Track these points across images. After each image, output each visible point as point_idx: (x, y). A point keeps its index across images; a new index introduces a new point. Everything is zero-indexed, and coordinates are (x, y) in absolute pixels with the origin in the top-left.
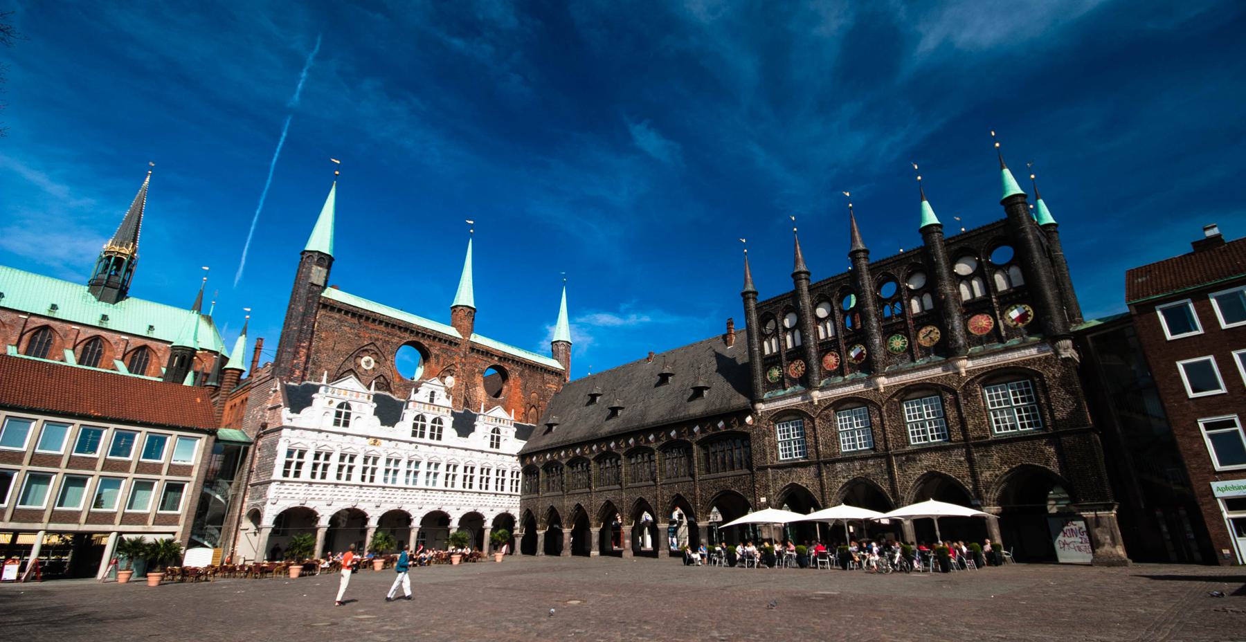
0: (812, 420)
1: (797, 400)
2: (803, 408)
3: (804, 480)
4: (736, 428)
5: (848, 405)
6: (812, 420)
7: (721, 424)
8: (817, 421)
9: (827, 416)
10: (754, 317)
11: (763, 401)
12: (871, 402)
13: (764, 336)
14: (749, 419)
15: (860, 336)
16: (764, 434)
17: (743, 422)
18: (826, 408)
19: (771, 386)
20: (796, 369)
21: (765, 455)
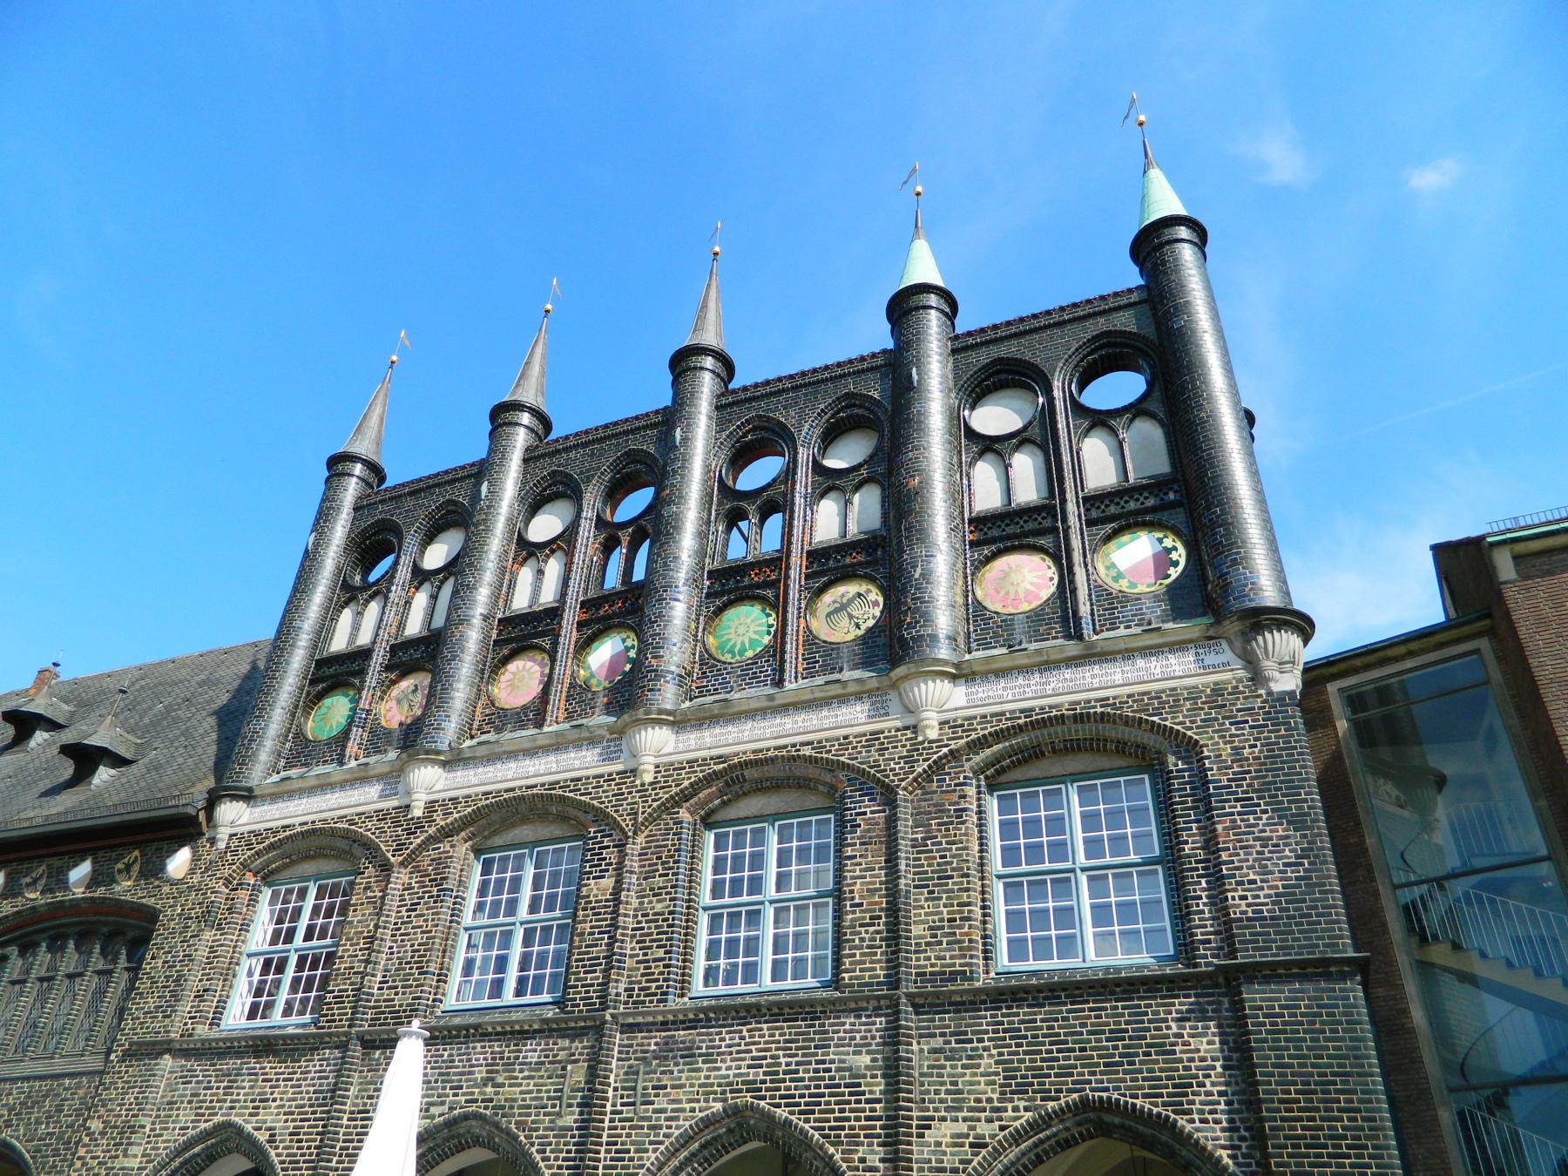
0: (386, 868)
1: (368, 797)
2: (367, 830)
3: (271, 1117)
4: (125, 888)
5: (525, 832)
6: (386, 868)
7: (81, 872)
8: (400, 877)
9: (441, 863)
10: (339, 532)
11: (248, 796)
12: (600, 816)
13: (349, 593)
14: (179, 862)
15: (630, 608)
16: (207, 917)
17: (153, 870)
18: (447, 833)
19: (301, 750)
20: (395, 706)
21: (176, 997)
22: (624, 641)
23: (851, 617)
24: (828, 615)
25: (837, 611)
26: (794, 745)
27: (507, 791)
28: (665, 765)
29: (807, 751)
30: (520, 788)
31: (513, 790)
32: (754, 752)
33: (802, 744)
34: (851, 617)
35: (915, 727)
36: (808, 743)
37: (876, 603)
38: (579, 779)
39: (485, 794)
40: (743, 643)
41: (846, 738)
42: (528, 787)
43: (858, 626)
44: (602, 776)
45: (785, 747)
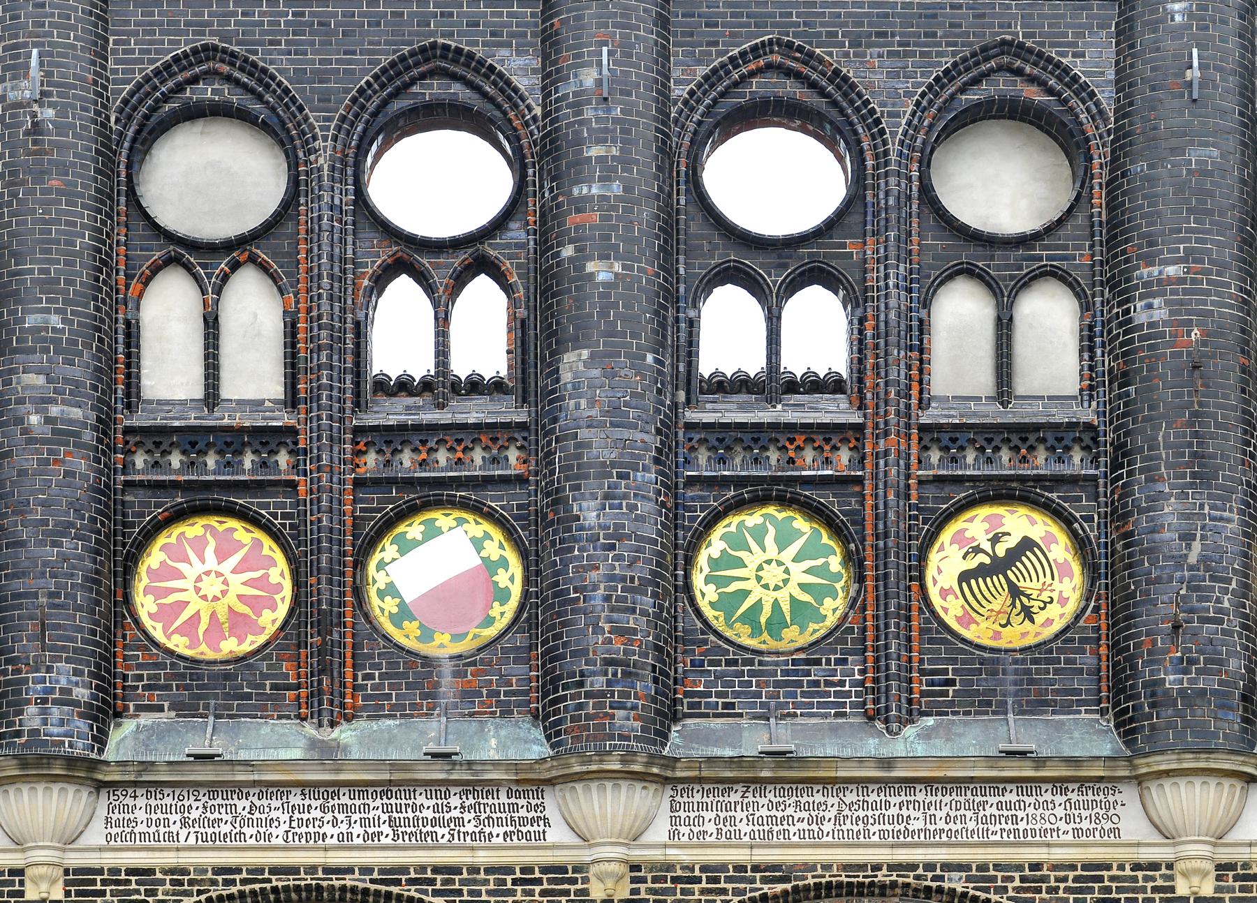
22: (478, 544)
23: (1015, 592)
24: (965, 577)
25: (982, 572)
26: (930, 867)
27: (275, 870)
28: (653, 867)
29: (956, 883)
30: (312, 869)
31: (293, 870)
32: (846, 867)
33: (947, 867)
34: (1015, 592)
35: (1170, 866)
36: (960, 867)
37: (1065, 571)
38: (456, 870)
39: (219, 870)
40: (776, 604)
41: (1036, 866)
42: (328, 870)
43: (1028, 614)
44: (508, 870)
45: (913, 867)
